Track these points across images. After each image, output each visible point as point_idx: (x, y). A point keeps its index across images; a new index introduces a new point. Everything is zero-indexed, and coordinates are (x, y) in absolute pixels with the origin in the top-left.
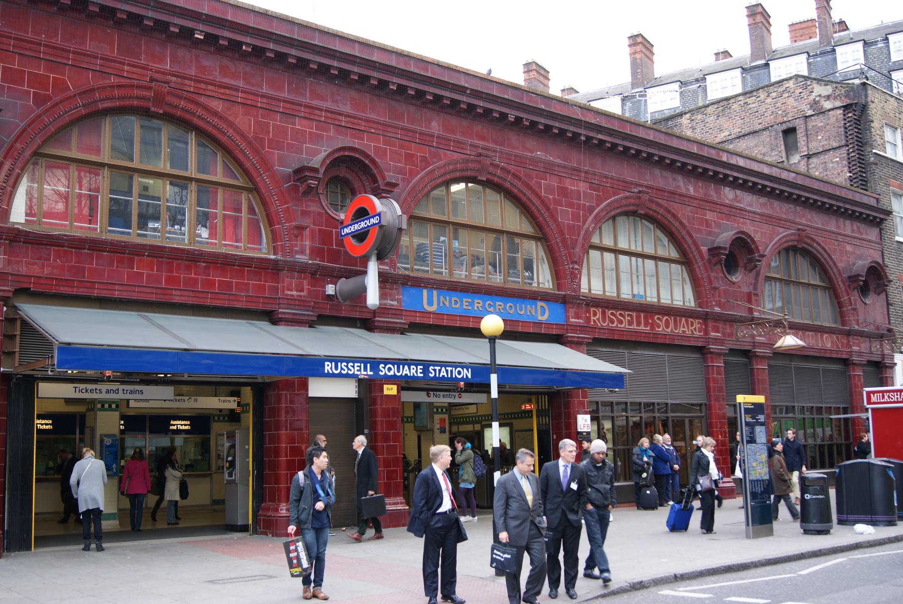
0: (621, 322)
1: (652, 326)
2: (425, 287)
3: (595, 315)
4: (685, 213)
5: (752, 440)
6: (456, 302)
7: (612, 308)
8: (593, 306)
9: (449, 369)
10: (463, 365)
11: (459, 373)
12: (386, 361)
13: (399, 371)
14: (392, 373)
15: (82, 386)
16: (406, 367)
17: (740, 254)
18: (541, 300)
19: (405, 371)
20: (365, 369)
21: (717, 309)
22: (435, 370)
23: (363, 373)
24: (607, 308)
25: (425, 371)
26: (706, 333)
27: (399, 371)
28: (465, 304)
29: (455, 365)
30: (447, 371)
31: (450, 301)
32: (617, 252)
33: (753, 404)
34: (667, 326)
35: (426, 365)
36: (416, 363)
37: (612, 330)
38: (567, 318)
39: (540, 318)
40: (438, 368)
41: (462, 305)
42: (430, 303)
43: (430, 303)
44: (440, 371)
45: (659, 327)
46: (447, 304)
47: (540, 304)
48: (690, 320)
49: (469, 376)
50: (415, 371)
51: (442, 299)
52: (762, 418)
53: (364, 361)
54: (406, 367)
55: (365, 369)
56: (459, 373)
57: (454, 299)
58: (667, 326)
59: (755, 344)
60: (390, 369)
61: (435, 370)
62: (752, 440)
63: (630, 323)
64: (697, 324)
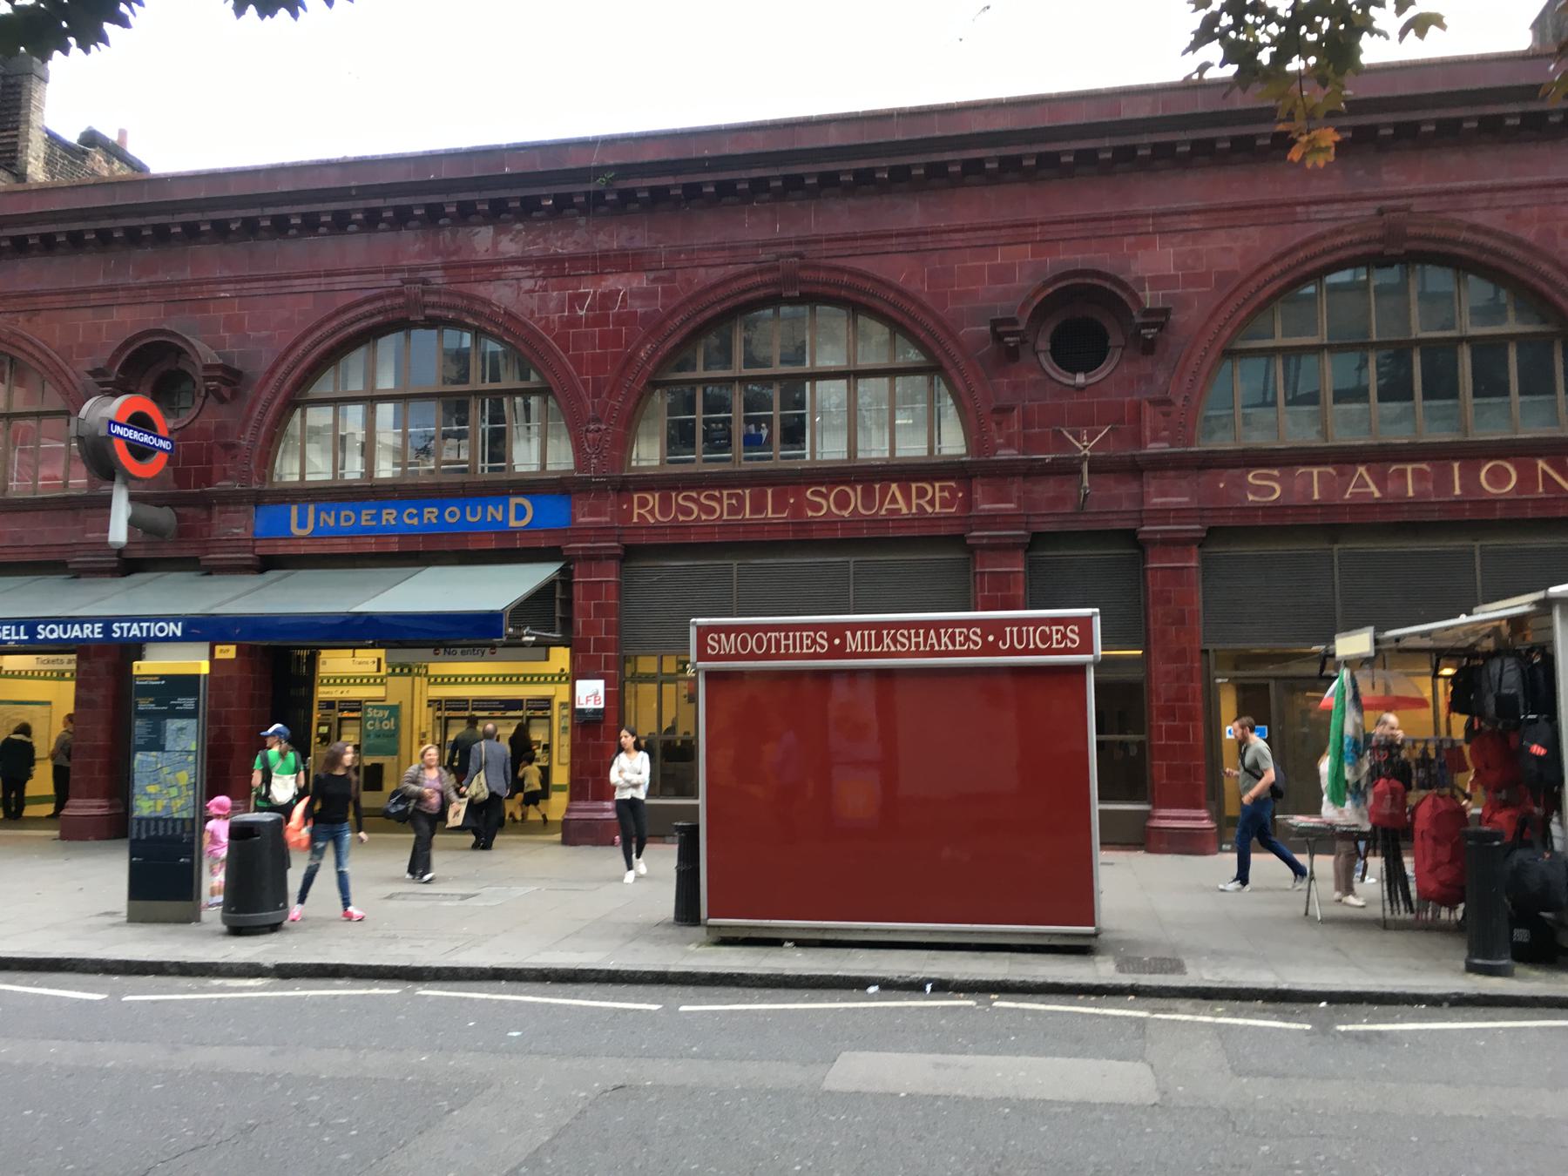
0: (711, 511)
1: (798, 510)
2: (294, 502)
3: (643, 503)
4: (897, 270)
5: (156, 744)
6: (348, 519)
7: (685, 488)
8: (637, 490)
9: (145, 625)
10: (168, 619)
11: (162, 630)
12: (47, 621)
13: (65, 632)
14: (55, 636)
15: (44, 657)
16: (77, 627)
17: (1085, 320)
18: (517, 494)
19: (75, 632)
20: (18, 633)
21: (1005, 454)
22: (121, 629)
23: (14, 637)
24: (676, 488)
25: (107, 630)
26: (968, 503)
27: (65, 632)
28: (364, 518)
29: (156, 619)
30: (141, 629)
31: (337, 518)
32: (852, 375)
33: (162, 677)
34: (843, 502)
35: (107, 623)
36: (92, 620)
37: (697, 526)
38: (573, 516)
39: (513, 523)
40: (125, 625)
41: (358, 519)
42: (302, 524)
43: (302, 524)
44: (129, 629)
45: (820, 507)
46: (332, 522)
47: (514, 501)
48: (914, 486)
49: (179, 633)
50: (93, 632)
51: (323, 515)
52: (188, 703)
53: (17, 622)
54: (77, 627)
55: (18, 633)
56: (162, 630)
57: (343, 514)
58: (843, 502)
59: (1144, 515)
60: (52, 631)
61: (121, 629)
62: (156, 744)
63: (733, 510)
64: (935, 490)
